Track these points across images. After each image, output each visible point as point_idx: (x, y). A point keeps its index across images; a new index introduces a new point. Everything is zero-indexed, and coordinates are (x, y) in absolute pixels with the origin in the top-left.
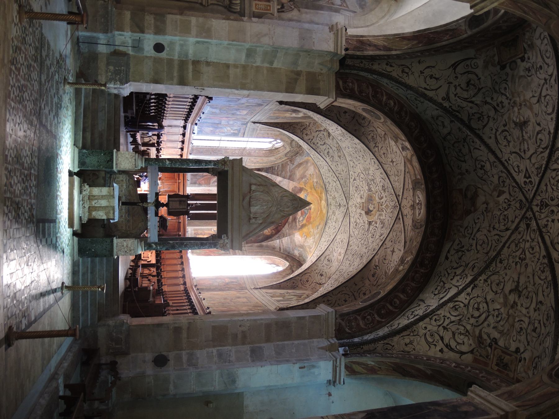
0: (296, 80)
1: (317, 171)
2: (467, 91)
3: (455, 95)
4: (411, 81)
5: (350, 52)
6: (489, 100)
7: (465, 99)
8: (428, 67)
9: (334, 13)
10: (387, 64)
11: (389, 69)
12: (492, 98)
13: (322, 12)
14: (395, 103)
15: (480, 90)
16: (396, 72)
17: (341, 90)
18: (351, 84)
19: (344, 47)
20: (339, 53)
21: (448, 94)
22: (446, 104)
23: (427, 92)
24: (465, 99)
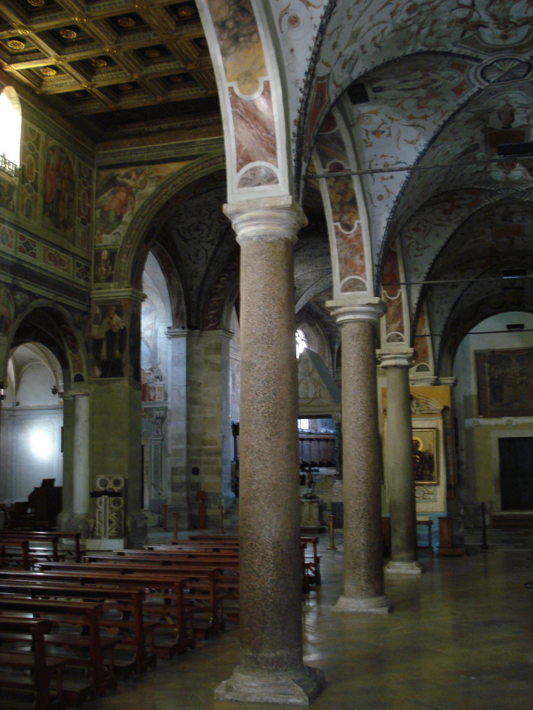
0: (212, 363)
1: (323, 294)
2: (203, 230)
3: (208, 237)
4: (202, 270)
5: (185, 324)
6: (207, 216)
7: (210, 230)
8: (190, 258)
9: (159, 335)
10: (192, 290)
11: (195, 288)
12: (206, 215)
13: (158, 345)
14: (224, 276)
15: (200, 223)
16: (197, 282)
17: (216, 325)
18: (211, 317)
19: (182, 330)
20: (186, 333)
21: (208, 242)
22: (216, 242)
23: (209, 257)
24: (210, 230)
